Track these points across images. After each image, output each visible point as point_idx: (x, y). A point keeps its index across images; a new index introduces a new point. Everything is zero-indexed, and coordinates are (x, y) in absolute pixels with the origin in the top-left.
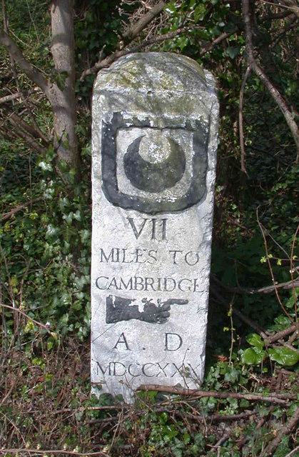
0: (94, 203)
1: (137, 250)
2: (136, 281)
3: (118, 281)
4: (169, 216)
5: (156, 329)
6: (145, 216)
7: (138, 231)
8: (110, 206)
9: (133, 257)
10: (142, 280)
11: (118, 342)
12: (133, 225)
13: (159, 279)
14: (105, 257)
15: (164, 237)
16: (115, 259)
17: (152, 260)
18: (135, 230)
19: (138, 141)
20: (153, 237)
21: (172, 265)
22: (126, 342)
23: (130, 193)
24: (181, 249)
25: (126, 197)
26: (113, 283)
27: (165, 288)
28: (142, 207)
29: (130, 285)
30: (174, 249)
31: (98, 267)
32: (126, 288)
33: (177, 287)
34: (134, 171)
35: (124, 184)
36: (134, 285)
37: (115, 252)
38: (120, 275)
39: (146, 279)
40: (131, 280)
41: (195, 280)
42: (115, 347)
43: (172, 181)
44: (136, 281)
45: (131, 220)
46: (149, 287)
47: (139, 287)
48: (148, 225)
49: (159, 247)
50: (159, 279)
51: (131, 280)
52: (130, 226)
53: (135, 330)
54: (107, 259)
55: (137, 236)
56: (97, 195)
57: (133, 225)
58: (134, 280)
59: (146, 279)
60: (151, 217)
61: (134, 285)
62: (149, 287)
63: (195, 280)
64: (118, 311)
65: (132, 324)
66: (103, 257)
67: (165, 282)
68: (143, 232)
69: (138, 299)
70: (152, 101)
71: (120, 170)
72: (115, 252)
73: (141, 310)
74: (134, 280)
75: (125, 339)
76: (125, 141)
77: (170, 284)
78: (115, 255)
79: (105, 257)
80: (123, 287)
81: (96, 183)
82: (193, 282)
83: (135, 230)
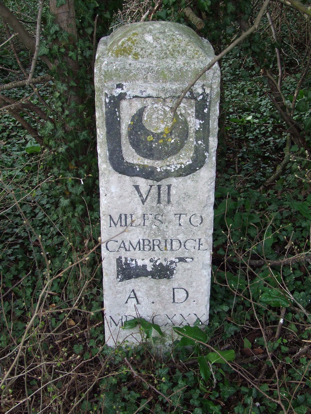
0: (100, 172)
1: (144, 215)
2: (144, 243)
3: (127, 244)
4: (174, 181)
5: (164, 286)
6: (150, 182)
7: (144, 197)
8: (116, 175)
9: (140, 221)
10: (150, 242)
11: (129, 298)
12: (139, 192)
13: (166, 241)
14: (114, 222)
15: (169, 202)
16: (123, 223)
17: (158, 223)
18: (141, 196)
19: (140, 113)
20: (159, 202)
21: (178, 227)
22: (136, 297)
23: (135, 162)
24: (186, 212)
25: (132, 166)
26: (122, 245)
27: (172, 248)
28: (148, 174)
29: (138, 246)
30: (179, 212)
31: (106, 231)
32: (135, 249)
33: (183, 246)
34: (139, 141)
35: (131, 156)
36: (142, 246)
37: (123, 217)
38: (128, 238)
39: (153, 241)
40: (139, 242)
41: (200, 239)
42: (126, 302)
43: (176, 150)
44: (144, 243)
45: (137, 187)
46: (156, 247)
47: (147, 248)
48: (154, 191)
49: (165, 211)
50: (166, 241)
51: (139, 242)
52: (136, 192)
53: (144, 287)
54: (116, 225)
55: (143, 202)
56: (104, 165)
57: (139, 192)
58: (141, 241)
59: (153, 241)
60: (156, 183)
61: (142, 246)
62: (156, 247)
63: (200, 239)
64: (127, 272)
65: (141, 281)
66: (112, 222)
67: (172, 243)
68: (149, 198)
69: (142, 259)
70: (153, 70)
71: (125, 140)
72: (123, 217)
73: (149, 269)
74: (141, 241)
75: (135, 294)
76: (127, 111)
77: (175, 244)
78: (124, 220)
79: (114, 222)
80: (131, 248)
81: (102, 151)
82: (198, 240)
83: (141, 196)
